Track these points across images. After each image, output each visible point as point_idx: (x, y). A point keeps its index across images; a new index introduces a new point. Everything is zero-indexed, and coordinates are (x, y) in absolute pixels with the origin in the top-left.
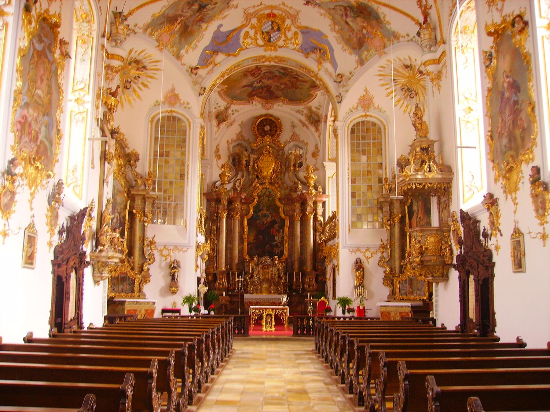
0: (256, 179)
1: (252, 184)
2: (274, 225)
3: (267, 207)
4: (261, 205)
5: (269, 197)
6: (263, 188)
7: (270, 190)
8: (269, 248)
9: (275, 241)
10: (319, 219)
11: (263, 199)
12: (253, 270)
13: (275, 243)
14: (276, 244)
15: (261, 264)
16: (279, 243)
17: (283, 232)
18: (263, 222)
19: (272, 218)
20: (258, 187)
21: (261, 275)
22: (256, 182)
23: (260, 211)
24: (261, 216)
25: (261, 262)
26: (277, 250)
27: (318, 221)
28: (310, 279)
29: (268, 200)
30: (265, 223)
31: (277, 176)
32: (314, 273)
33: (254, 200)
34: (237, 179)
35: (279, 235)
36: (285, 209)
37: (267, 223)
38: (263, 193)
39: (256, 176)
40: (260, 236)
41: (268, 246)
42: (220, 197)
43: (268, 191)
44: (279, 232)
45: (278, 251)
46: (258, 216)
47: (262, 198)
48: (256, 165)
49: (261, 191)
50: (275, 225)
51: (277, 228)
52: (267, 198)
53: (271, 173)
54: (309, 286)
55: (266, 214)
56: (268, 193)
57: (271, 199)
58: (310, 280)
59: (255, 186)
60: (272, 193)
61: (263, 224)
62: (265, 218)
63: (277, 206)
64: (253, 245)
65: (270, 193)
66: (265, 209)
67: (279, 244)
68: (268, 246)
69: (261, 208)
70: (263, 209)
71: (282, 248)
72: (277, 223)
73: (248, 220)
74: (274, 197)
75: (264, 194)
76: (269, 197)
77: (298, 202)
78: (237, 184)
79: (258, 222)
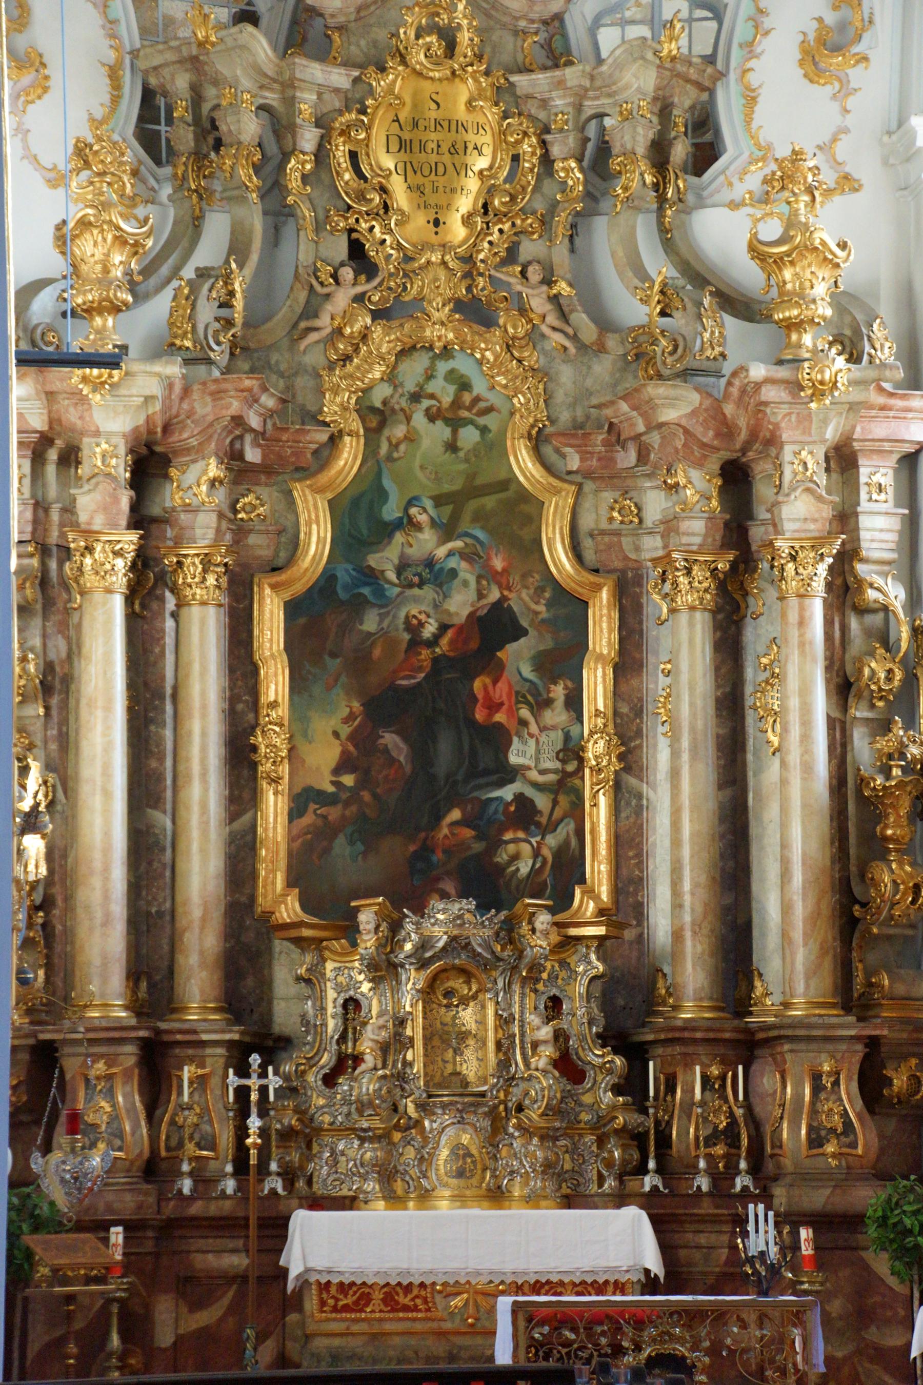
0: (347, 273)
1: (311, 311)
2: (501, 647)
3: (439, 501)
4: (387, 483)
5: (455, 424)
6: (405, 353)
7: (462, 364)
8: (468, 833)
9: (509, 774)
10: (872, 594)
11: (411, 438)
12: (351, 1005)
13: (507, 793)
14: (520, 798)
15: (423, 965)
16: (536, 785)
17: (574, 702)
18: (413, 627)
19: (481, 596)
20: (364, 337)
21: (415, 1055)
22: (342, 299)
23: (386, 531)
24: (392, 576)
25: (424, 944)
26: (526, 849)
27: (862, 611)
28: (816, 1078)
29: (452, 447)
30: (429, 630)
31: (511, 256)
32: (849, 1027)
33: (334, 440)
34: (203, 273)
35: (542, 729)
36: (587, 521)
37: (443, 628)
38: (410, 386)
39: (340, 249)
40: (390, 739)
41: (456, 814)
42: (72, 416)
43: (443, 367)
44: (542, 704)
45: (536, 853)
46: (372, 577)
47: (399, 431)
48: (340, 152)
49: (391, 378)
50: (512, 647)
51: (527, 671)
52: (442, 431)
53: (467, 220)
54: (816, 1140)
55: (430, 563)
56: (446, 393)
57: (469, 436)
58: (817, 1089)
59: (339, 331)
60: (479, 387)
61: (416, 643)
62: (428, 593)
63: (524, 496)
64: (334, 813)
65: (464, 385)
66: (423, 518)
67: (542, 802)
68: (456, 814)
69: (391, 511)
70: (407, 523)
71: (566, 829)
72: (524, 633)
73: (292, 609)
74: (491, 421)
75: (415, 397)
76: (455, 424)
77: (699, 464)
78: (206, 312)
79: (370, 623)
